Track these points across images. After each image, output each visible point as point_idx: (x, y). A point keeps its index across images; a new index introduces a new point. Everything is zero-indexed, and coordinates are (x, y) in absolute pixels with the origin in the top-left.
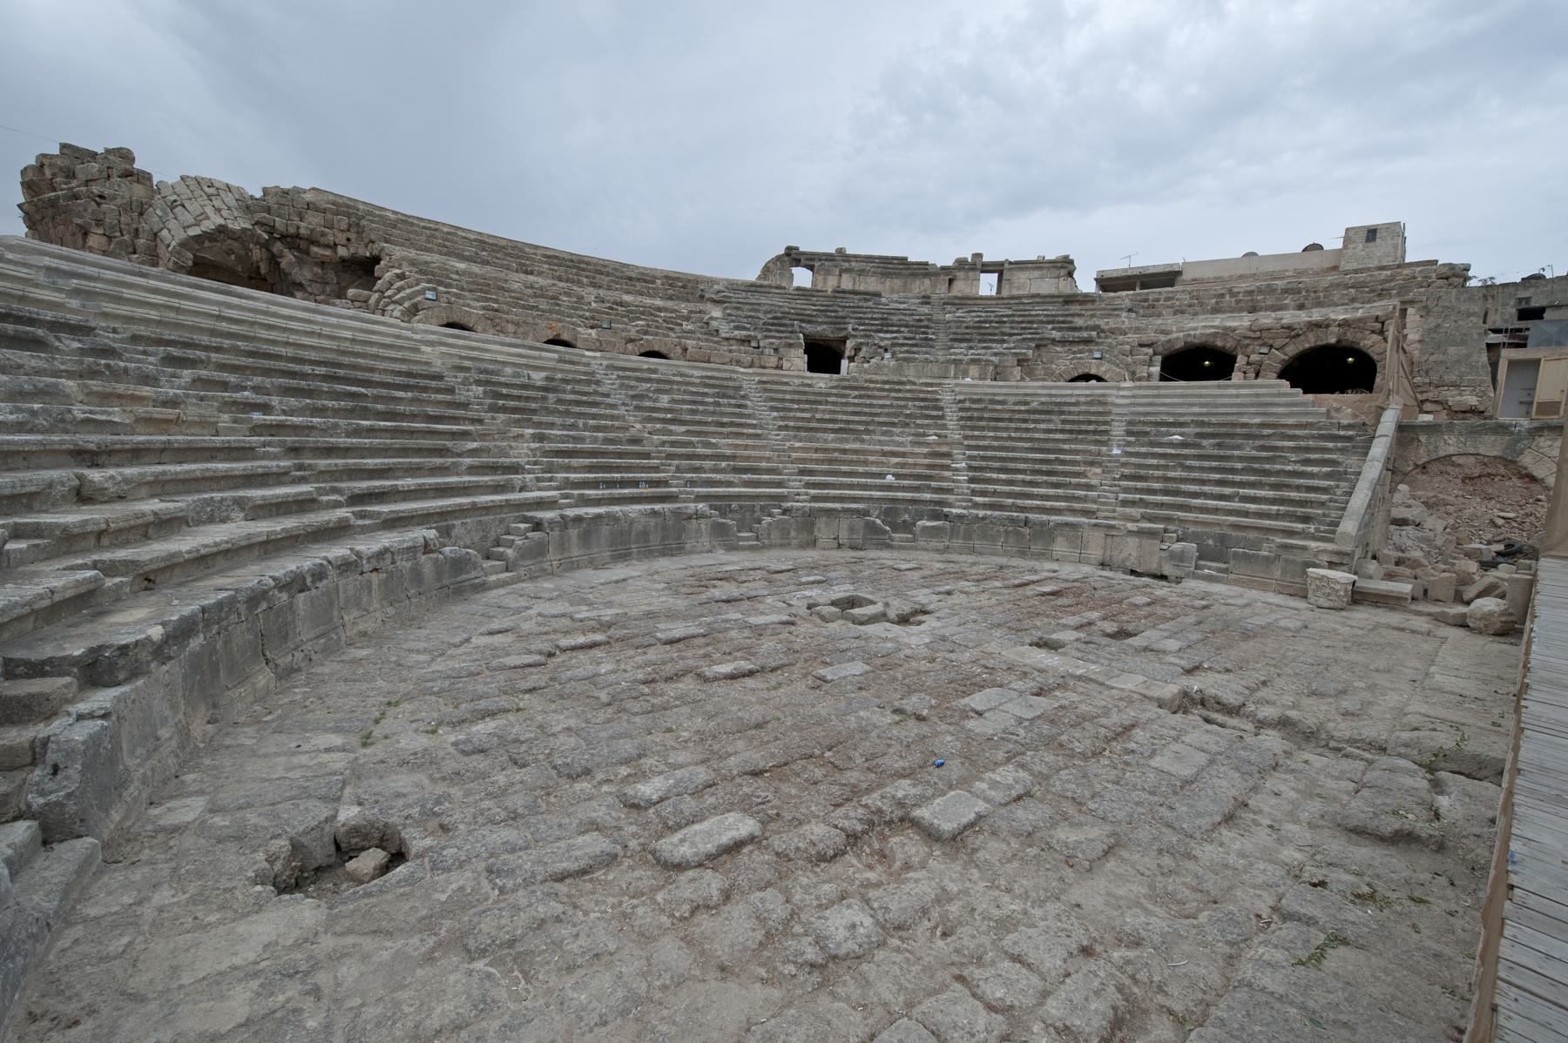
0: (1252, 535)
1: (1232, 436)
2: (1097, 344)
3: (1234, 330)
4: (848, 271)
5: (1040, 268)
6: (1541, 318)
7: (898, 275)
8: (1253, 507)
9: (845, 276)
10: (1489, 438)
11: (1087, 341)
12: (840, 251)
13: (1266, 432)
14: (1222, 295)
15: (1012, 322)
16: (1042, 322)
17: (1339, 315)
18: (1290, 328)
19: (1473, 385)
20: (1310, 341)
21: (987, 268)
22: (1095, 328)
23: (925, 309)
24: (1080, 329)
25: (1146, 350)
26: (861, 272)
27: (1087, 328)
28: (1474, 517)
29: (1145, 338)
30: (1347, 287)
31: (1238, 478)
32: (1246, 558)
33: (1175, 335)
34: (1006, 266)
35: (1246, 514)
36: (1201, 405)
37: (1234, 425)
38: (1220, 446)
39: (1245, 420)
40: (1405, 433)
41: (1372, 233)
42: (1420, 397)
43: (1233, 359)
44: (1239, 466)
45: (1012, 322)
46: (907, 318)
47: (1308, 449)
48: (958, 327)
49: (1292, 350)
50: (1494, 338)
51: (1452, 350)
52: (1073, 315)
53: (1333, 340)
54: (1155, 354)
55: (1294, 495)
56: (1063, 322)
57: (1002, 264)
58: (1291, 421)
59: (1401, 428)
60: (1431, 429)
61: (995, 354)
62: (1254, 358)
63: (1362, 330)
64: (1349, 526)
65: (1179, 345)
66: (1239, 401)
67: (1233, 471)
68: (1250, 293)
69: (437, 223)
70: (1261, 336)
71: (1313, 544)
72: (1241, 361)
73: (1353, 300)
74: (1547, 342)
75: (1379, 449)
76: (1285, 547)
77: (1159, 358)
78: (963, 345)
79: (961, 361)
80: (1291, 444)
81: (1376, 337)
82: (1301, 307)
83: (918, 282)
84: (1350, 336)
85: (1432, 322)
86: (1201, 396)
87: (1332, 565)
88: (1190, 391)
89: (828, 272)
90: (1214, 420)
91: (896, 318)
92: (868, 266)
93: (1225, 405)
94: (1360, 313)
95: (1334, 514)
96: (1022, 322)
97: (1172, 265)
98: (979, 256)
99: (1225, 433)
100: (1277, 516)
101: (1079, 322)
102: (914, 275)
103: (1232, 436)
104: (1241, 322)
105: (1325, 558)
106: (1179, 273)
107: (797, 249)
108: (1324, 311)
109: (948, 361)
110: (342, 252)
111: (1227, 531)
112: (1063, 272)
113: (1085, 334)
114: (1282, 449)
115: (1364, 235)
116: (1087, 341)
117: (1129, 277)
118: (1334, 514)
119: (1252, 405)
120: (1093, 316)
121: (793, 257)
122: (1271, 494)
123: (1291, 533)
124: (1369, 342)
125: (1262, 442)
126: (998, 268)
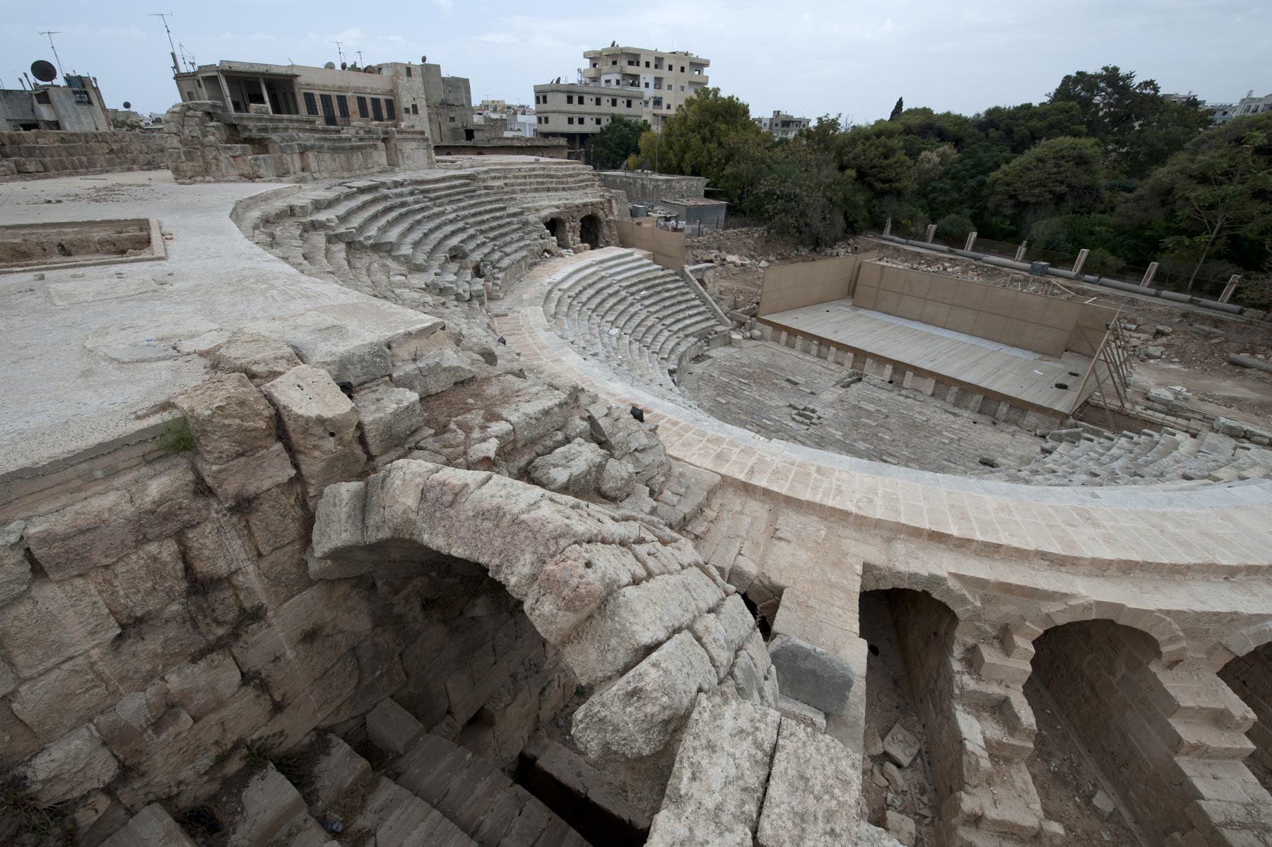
5: (414, 140)
18: (577, 207)
72: (567, 224)
106: (297, 76)
115: (404, 71)
117: (256, 73)
124: (601, 214)
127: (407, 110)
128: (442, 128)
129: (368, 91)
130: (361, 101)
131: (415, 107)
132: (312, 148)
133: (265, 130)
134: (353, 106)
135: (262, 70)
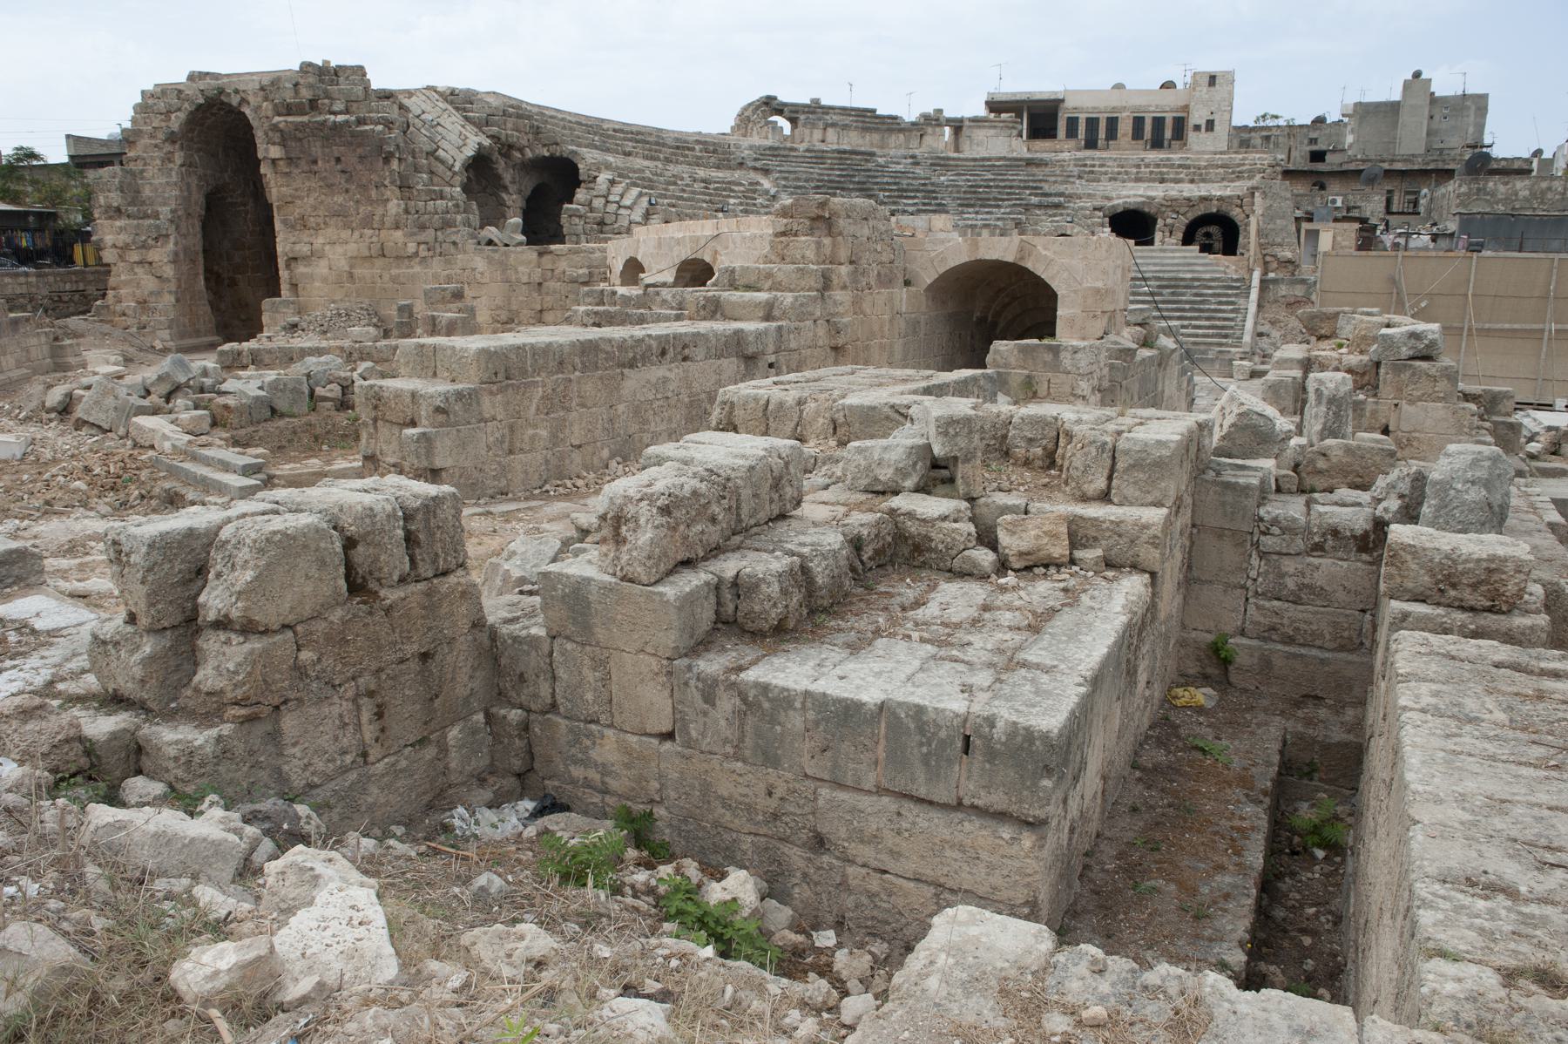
0: (1202, 347)
1: (1177, 287)
2: (1065, 208)
3: (1153, 198)
4: (833, 125)
5: (995, 127)
6: (1324, 160)
7: (877, 130)
8: (1200, 331)
9: (831, 132)
10: (1299, 286)
11: (1057, 206)
12: (816, 101)
13: (1196, 284)
14: (1138, 166)
15: (997, 187)
16: (1019, 187)
17: (1216, 190)
18: (1188, 199)
19: (1289, 244)
20: (1200, 211)
21: (949, 121)
22: (1061, 194)
23: (918, 170)
24: (1050, 195)
25: (1097, 213)
26: (845, 127)
27: (1056, 195)
28: (1293, 329)
29: (1098, 203)
30: (1218, 167)
31: (1189, 314)
32: (1202, 360)
33: (1116, 202)
34: (967, 123)
35: (1197, 336)
36: (1155, 265)
37: (1176, 279)
38: (1173, 294)
39: (1181, 275)
40: (1264, 283)
41: (1212, 80)
42: (1264, 252)
43: (1155, 221)
44: (1187, 306)
45: (997, 187)
46: (914, 182)
47: (1219, 295)
48: (958, 192)
49: (1191, 216)
50: (1299, 213)
51: (1278, 221)
52: (1040, 181)
53: (1214, 210)
54: (1105, 216)
55: (1218, 323)
56: (1036, 188)
57: (961, 120)
58: (1208, 276)
59: (1262, 281)
60: (1275, 281)
61: (998, 219)
62: (1169, 221)
63: (1231, 204)
64: (1247, 338)
65: (1120, 210)
66: (1176, 261)
67: (1183, 310)
68: (1158, 166)
69: (539, 106)
70: (1172, 204)
71: (1233, 349)
72: (1160, 222)
73: (1223, 179)
74: (1322, 220)
75: (1254, 294)
76: (1220, 352)
77: (1107, 220)
78: (971, 210)
79: (976, 226)
80: (1210, 292)
81: (1238, 210)
82: (1192, 181)
83: (893, 137)
84: (1224, 208)
85: (1268, 203)
86: (1152, 258)
87: (1241, 359)
88: (1145, 254)
89: (814, 126)
90: (1166, 275)
91: (905, 182)
92: (848, 120)
93: (1168, 265)
94: (1228, 192)
95: (1238, 332)
96: (1005, 187)
97: (1056, 93)
98: (940, 111)
99: (1175, 284)
100: (1212, 336)
101: (1046, 188)
102: (890, 130)
103: (1177, 287)
104: (1158, 192)
105: (1238, 356)
106: (1063, 101)
107: (775, 98)
108: (1208, 186)
109: (967, 226)
110: (529, 154)
111: (1190, 346)
112: (1015, 132)
113: (1056, 200)
114: (1206, 295)
115: (1207, 80)
116: (1057, 206)
117: (1017, 101)
118: (1238, 332)
119: (1184, 265)
120: (1055, 182)
121: (770, 105)
122: (1207, 323)
123: (1221, 345)
124: (1236, 213)
125: (1194, 291)
126: (958, 126)
127: (1197, 128)
128: (1293, 154)
129: (1152, 109)
130: (1138, 122)
131: (1210, 125)
132: (833, 125)
133: (797, 112)
134: (1125, 128)
135: (1024, 97)
